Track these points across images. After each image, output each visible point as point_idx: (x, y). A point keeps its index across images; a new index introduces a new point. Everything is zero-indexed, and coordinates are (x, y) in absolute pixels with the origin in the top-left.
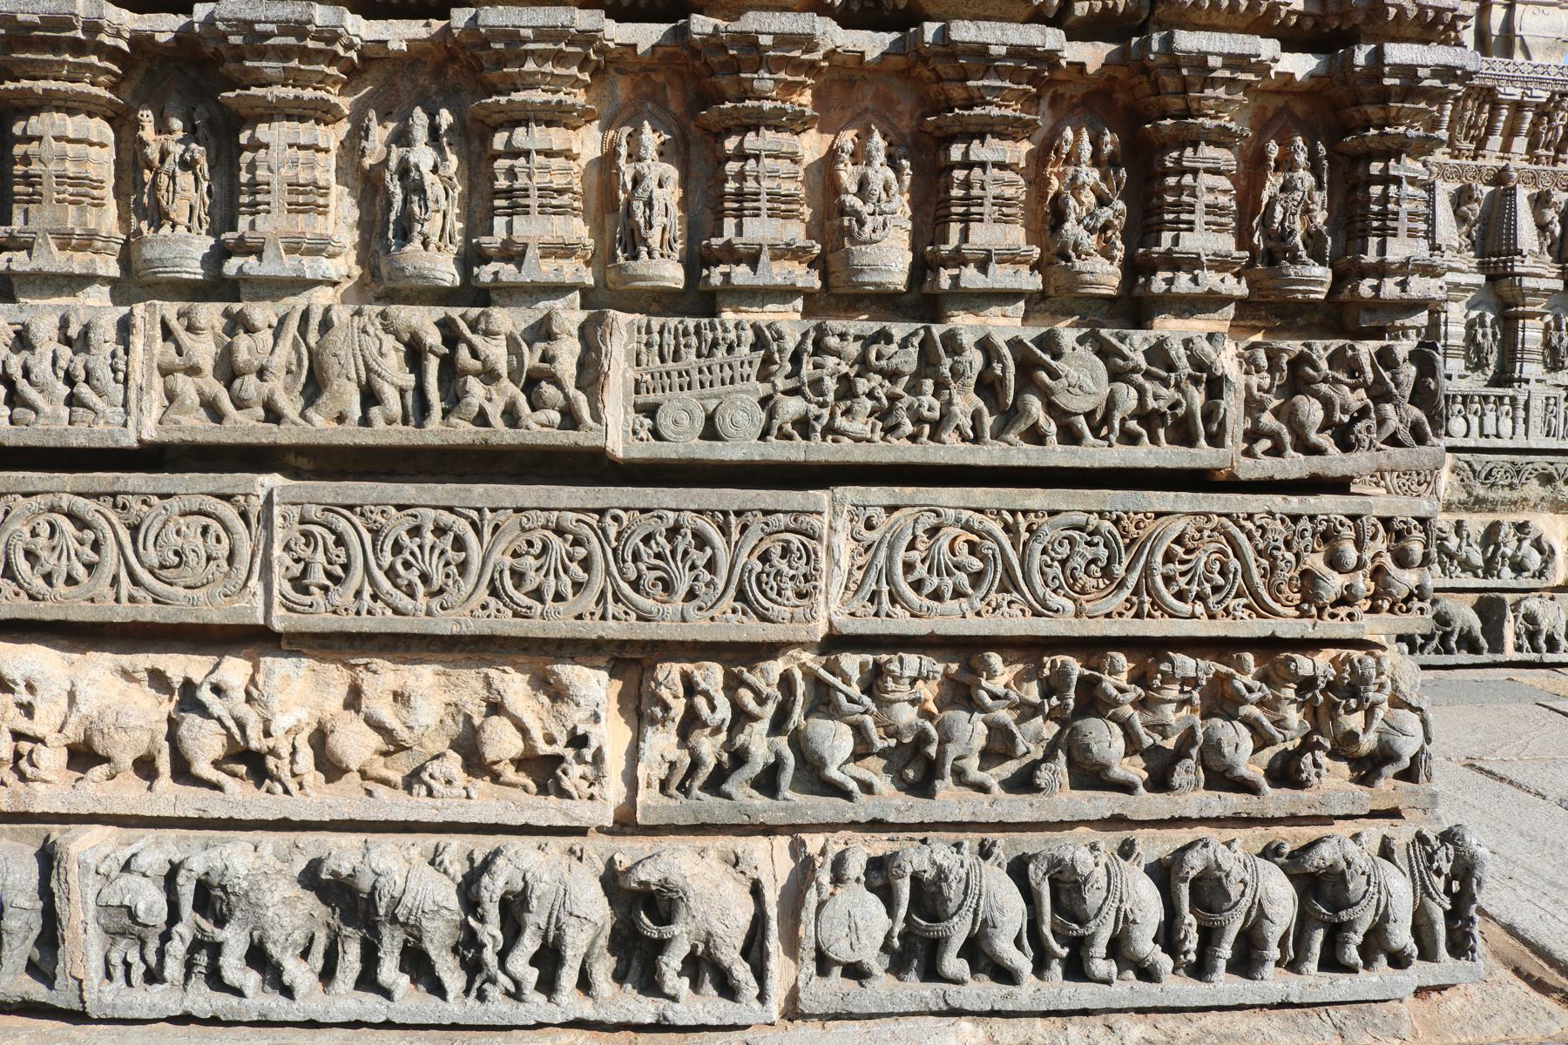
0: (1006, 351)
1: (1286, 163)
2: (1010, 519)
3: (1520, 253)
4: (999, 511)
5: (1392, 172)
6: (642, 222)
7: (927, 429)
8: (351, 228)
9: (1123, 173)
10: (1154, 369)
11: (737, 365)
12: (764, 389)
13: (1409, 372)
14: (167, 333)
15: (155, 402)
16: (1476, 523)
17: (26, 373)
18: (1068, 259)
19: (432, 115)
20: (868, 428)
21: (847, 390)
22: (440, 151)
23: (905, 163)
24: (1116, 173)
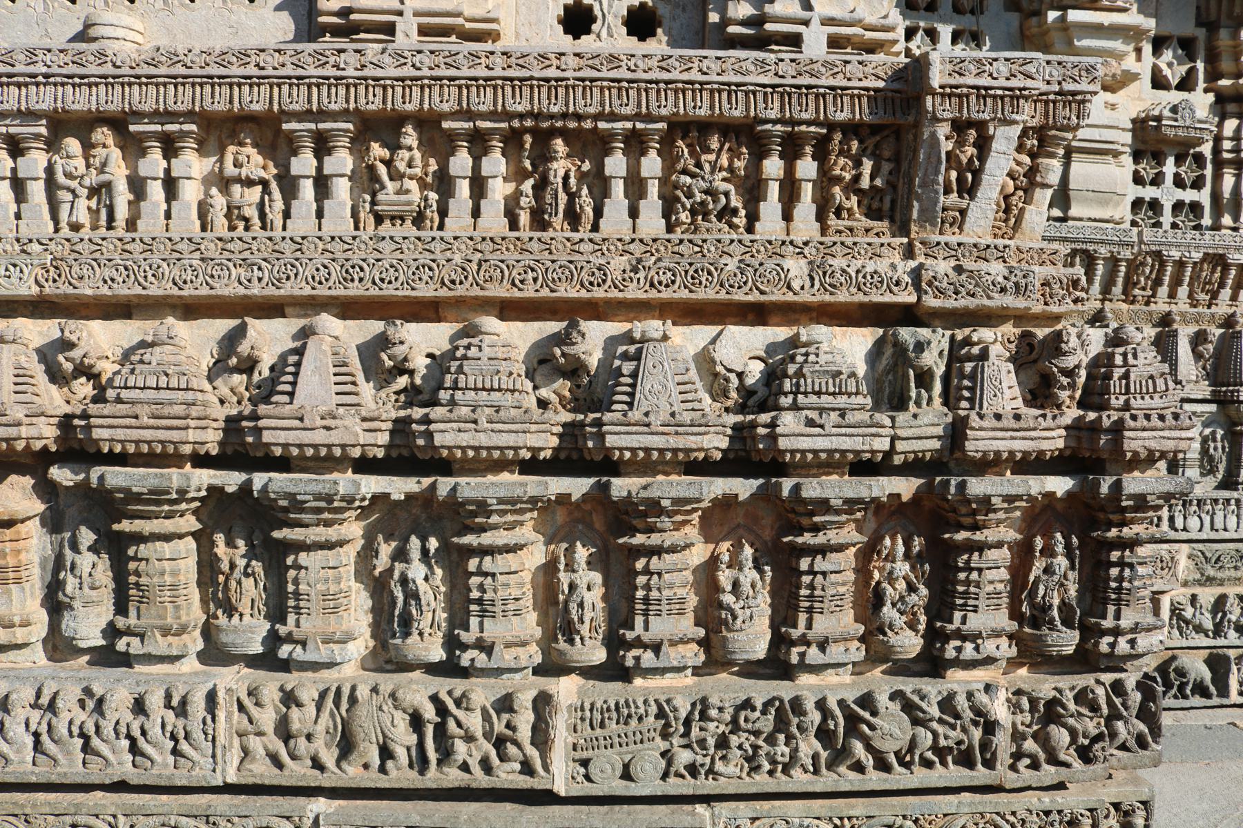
0: (838, 712)
1: (1048, 552)
4: (830, 819)
5: (1127, 560)
6: (576, 619)
7: (780, 767)
8: (366, 613)
9: (927, 567)
10: (945, 717)
12: (663, 745)
13: (1136, 697)
15: (235, 755)
16: (1207, 595)
17: (144, 733)
18: (885, 634)
19: (424, 540)
20: (738, 770)
21: (722, 743)
22: (430, 567)
23: (767, 568)
24: (922, 566)
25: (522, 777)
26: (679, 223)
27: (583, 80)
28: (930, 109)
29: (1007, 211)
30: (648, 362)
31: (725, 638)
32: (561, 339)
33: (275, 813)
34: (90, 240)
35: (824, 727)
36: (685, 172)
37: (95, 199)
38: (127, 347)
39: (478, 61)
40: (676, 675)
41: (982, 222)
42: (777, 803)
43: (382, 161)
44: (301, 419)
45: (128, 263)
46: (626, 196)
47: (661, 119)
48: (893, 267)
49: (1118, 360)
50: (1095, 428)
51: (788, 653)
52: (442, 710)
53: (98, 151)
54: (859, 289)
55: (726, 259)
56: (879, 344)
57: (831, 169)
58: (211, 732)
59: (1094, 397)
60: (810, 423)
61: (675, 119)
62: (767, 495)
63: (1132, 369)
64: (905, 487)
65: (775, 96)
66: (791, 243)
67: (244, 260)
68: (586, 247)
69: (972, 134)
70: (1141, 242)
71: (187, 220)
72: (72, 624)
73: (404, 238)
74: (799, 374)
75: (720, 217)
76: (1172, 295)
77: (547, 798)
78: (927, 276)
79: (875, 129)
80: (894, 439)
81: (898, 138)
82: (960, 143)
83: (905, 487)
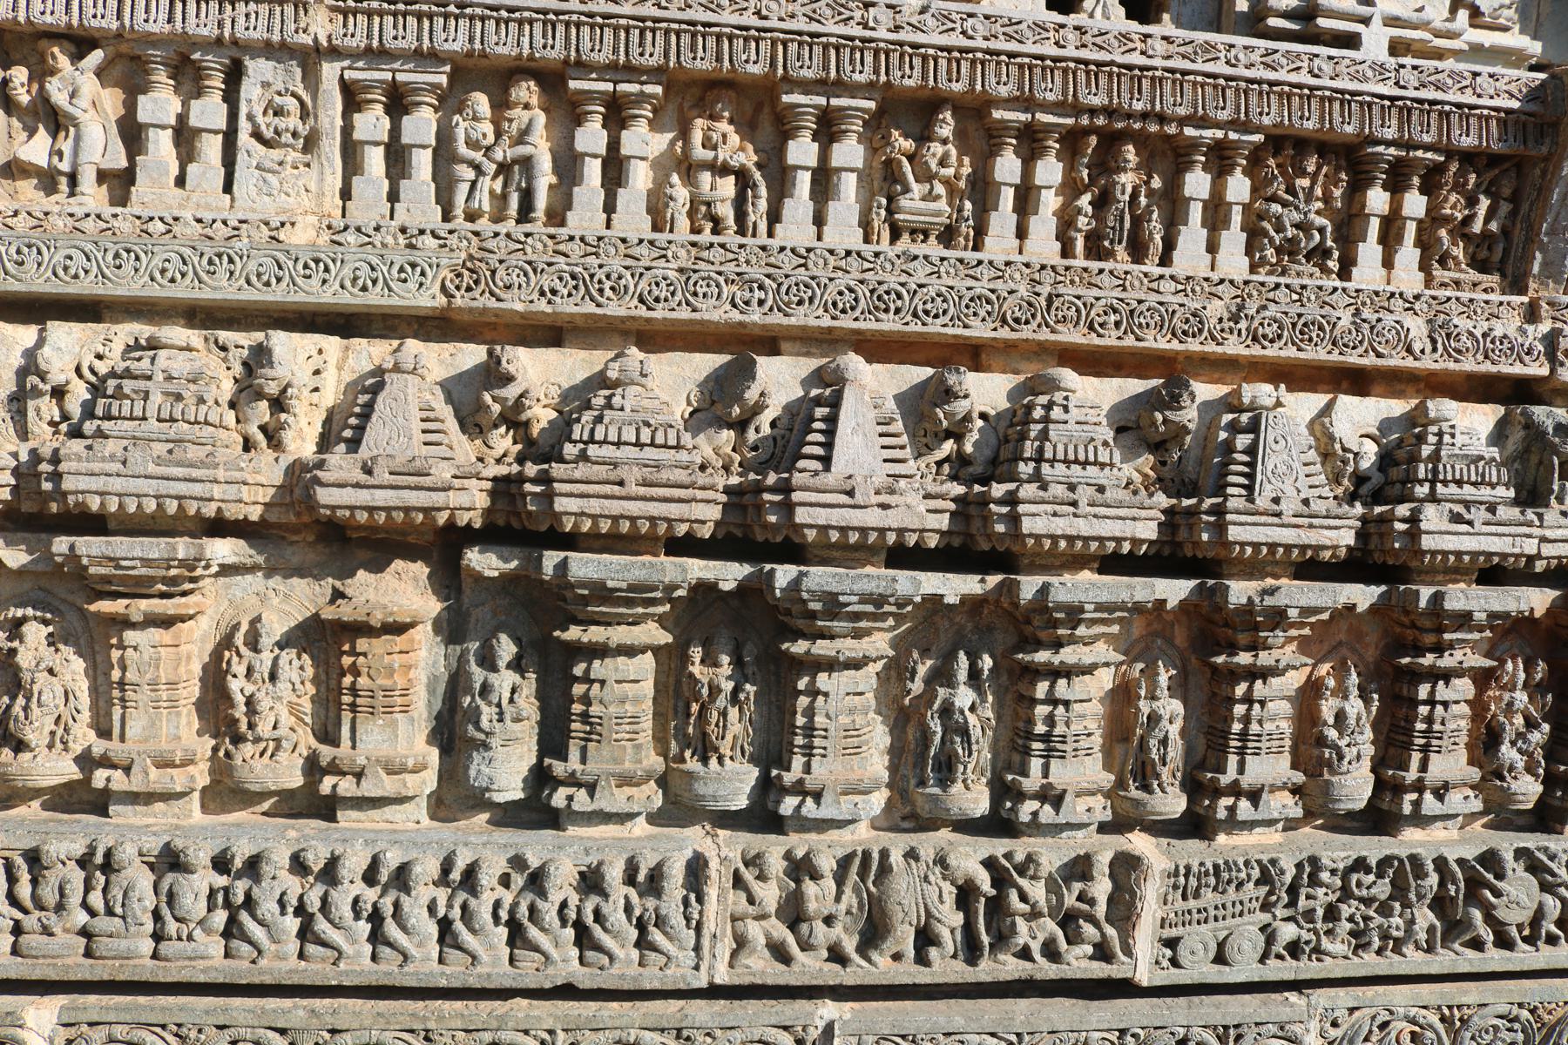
2: (1446, 1011)
4: (1439, 1008)
8: (882, 754)
9: (1550, 696)
11: (1246, 901)
15: (726, 945)
17: (598, 916)
18: (1502, 779)
21: (1332, 913)
24: (1544, 696)
25: (1096, 964)
26: (1263, 261)
27: (1172, 71)
30: (1269, 435)
31: (1328, 782)
32: (1149, 401)
33: (773, 1022)
34: (508, 235)
37: (500, 179)
38: (566, 385)
39: (1045, 35)
40: (1267, 830)
42: (1381, 989)
44: (851, 493)
45: (578, 269)
46: (1204, 225)
47: (1258, 129)
52: (1001, 879)
53: (517, 112)
54: (1486, 357)
58: (696, 916)
60: (1456, 518)
61: (1278, 131)
67: (738, 274)
72: (486, 770)
74: (1435, 457)
75: (1308, 257)
77: (1125, 988)
79: (1493, 160)
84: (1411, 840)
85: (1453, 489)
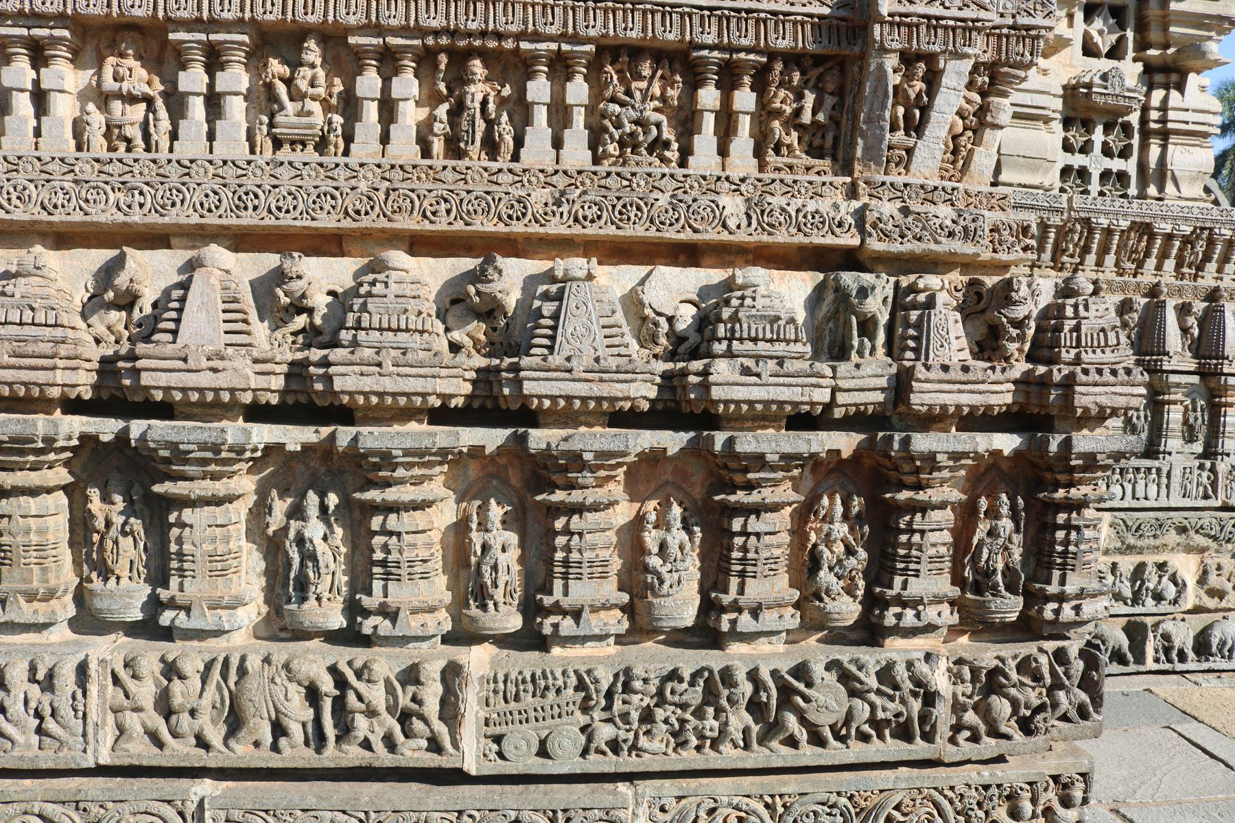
0: (771, 683)
1: (993, 513)
2: (769, 800)
3: (1167, 354)
4: (761, 796)
5: (1074, 523)
6: (489, 583)
7: (708, 742)
9: (866, 529)
10: (883, 688)
11: (563, 704)
12: (583, 719)
13: (1079, 666)
14: (116, 680)
15: (110, 733)
16: (1127, 564)
18: (821, 600)
19: (322, 495)
20: (663, 746)
21: (647, 717)
22: (329, 526)
23: (696, 529)
24: (861, 527)
25: (430, 755)
26: (606, 155)
28: (878, 38)
29: (955, 152)
30: (571, 302)
31: (650, 603)
32: (476, 276)
35: (756, 700)
36: (613, 100)
40: (598, 644)
41: (930, 163)
42: (705, 781)
43: (281, 79)
44: (185, 360)
46: (550, 125)
47: (589, 41)
48: (836, 207)
49: (1069, 312)
50: (1045, 383)
51: (718, 620)
52: (341, 683)
54: (799, 230)
55: (656, 194)
56: (819, 290)
57: (771, 102)
58: (81, 707)
59: (1042, 351)
60: (746, 371)
61: (604, 42)
62: (697, 450)
63: (1083, 322)
64: (845, 443)
65: (713, 19)
66: (727, 179)
67: (123, 183)
68: (505, 178)
69: (921, 68)
70: (1071, 208)
71: (58, 138)
73: (305, 164)
74: (735, 318)
76: (1099, 263)
77: (457, 777)
78: (871, 217)
79: (818, 60)
80: (835, 390)
81: (843, 71)
82: (908, 77)
83: (845, 443)
84: (896, 649)
85: (749, 345)
